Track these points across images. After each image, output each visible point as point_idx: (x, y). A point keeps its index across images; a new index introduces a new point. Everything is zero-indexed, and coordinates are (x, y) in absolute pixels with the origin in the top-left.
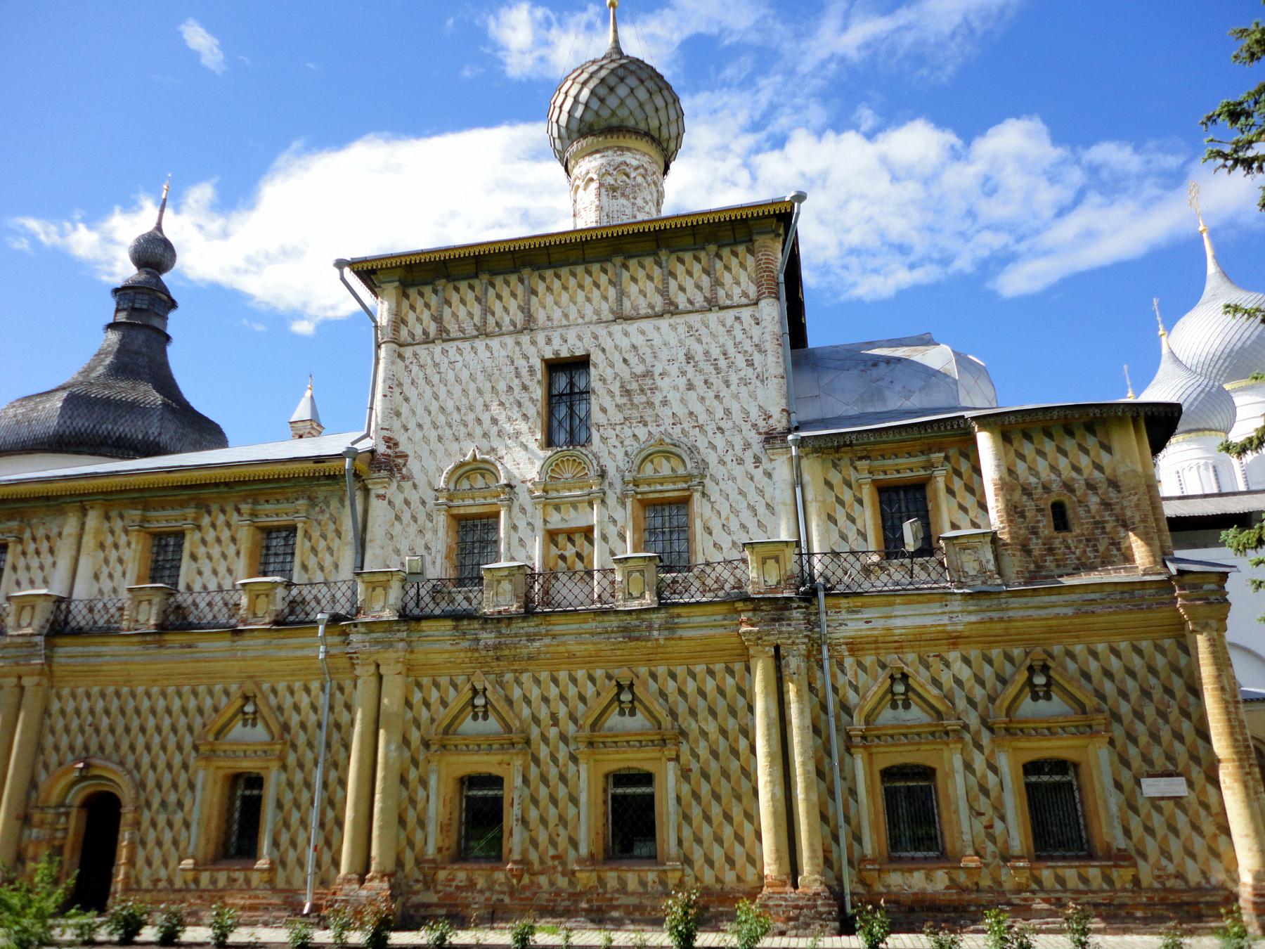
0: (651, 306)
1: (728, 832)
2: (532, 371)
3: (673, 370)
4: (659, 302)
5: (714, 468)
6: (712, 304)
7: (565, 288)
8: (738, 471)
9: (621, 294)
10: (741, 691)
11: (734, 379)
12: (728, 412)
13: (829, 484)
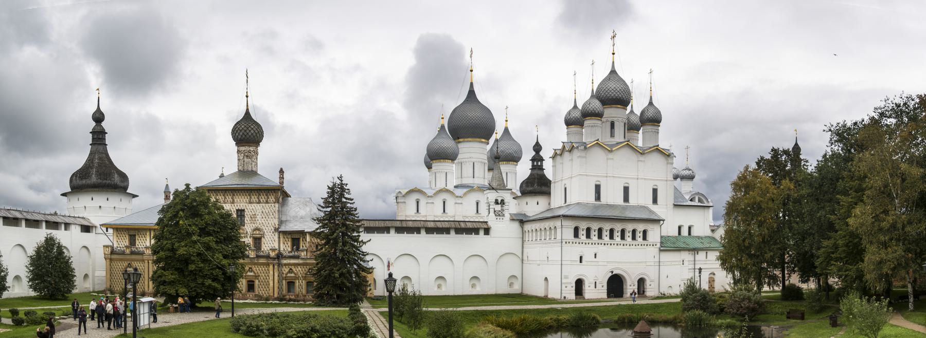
0: (256, 201)
1: (265, 289)
2: (234, 211)
3: (259, 214)
4: (257, 200)
5: (266, 232)
6: (267, 202)
7: (240, 195)
8: (270, 234)
9: (251, 198)
10: (268, 270)
11: (270, 217)
12: (269, 223)
13: (284, 238)
